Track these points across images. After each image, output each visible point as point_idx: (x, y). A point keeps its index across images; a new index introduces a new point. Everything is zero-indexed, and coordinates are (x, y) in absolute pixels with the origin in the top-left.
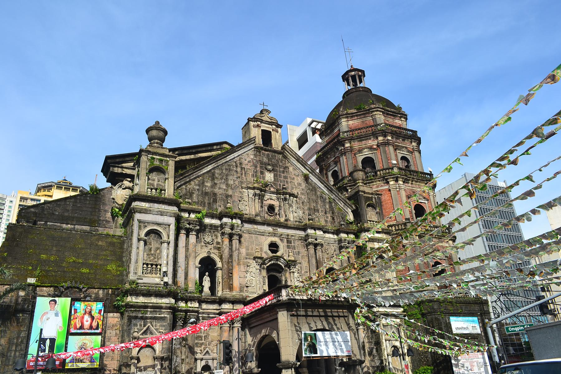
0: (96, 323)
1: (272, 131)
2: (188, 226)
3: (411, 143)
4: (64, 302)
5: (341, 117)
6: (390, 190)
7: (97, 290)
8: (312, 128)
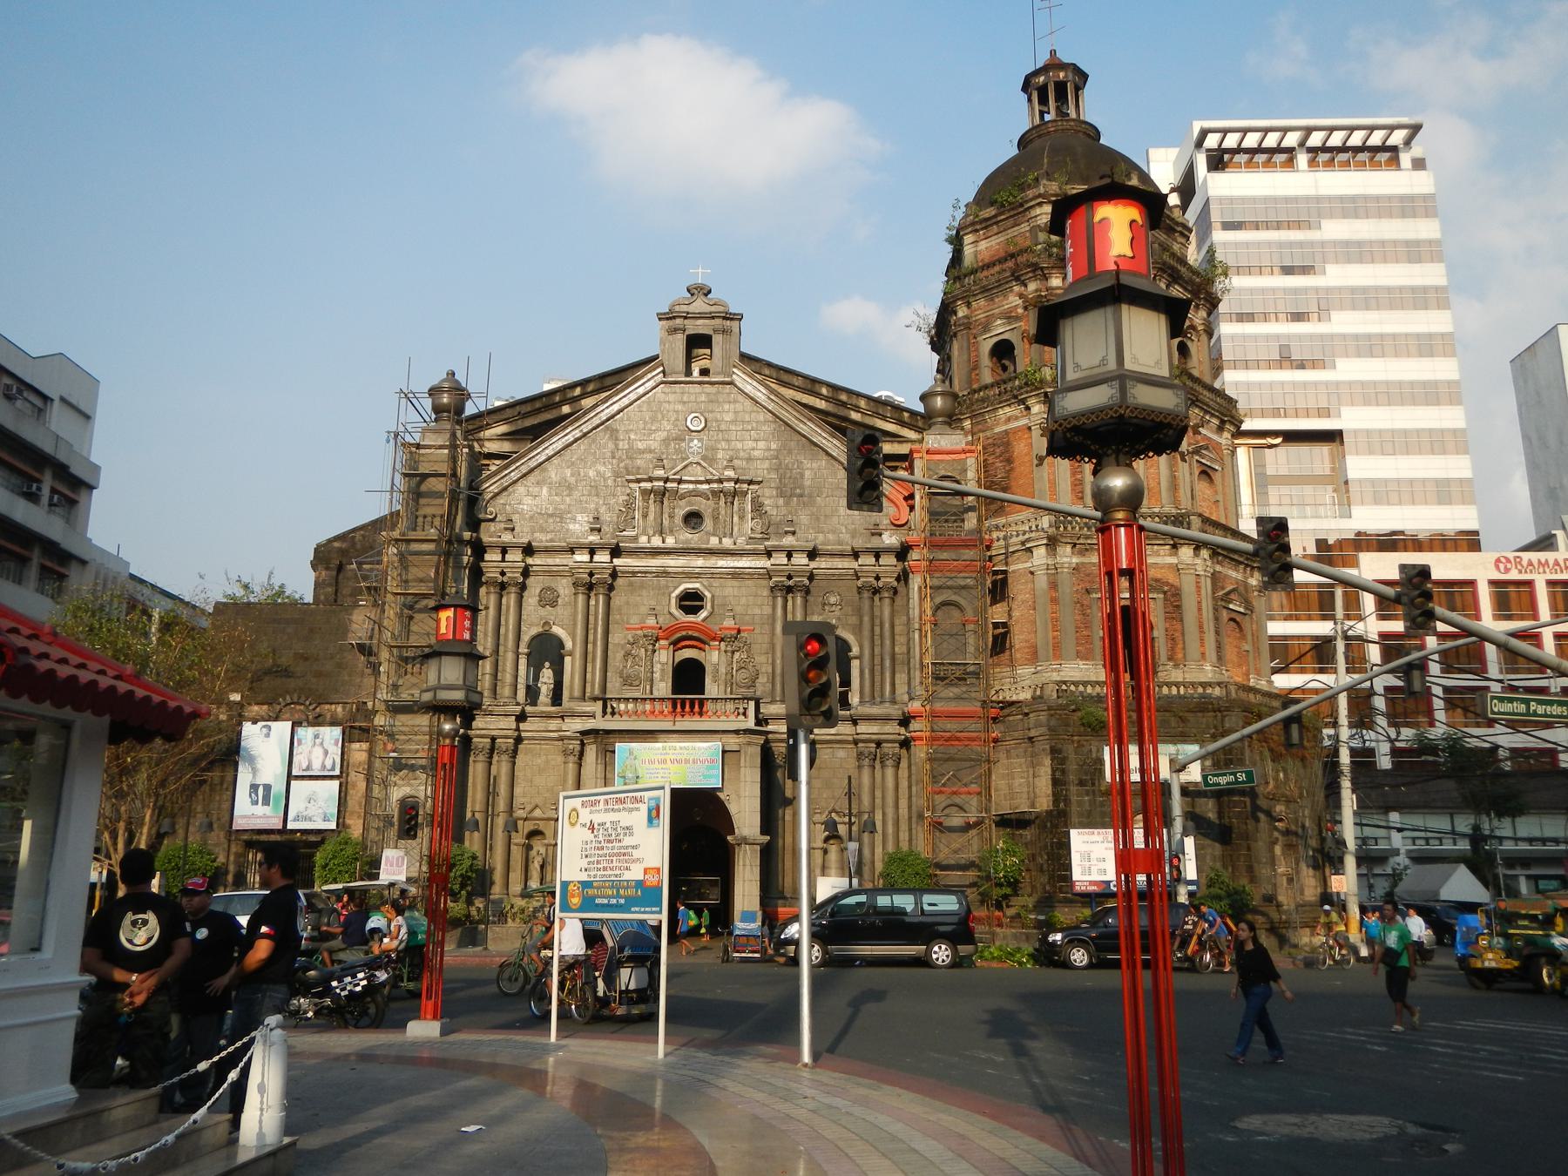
0: (332, 760)
1: (711, 332)
2: (500, 579)
4: (282, 728)
6: (1030, 428)
7: (333, 706)
8: (1208, 150)
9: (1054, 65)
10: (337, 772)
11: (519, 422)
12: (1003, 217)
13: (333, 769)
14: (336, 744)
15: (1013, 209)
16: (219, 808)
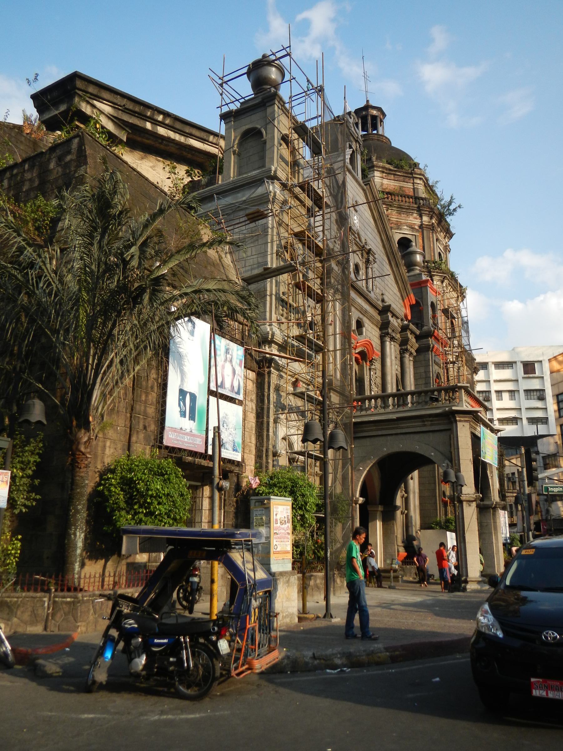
3: (445, 238)
5: (375, 169)
9: (367, 107)
10: (241, 397)
11: (120, 112)
12: (399, 174)
13: (238, 393)
14: (240, 366)
15: (406, 173)
16: (145, 414)
